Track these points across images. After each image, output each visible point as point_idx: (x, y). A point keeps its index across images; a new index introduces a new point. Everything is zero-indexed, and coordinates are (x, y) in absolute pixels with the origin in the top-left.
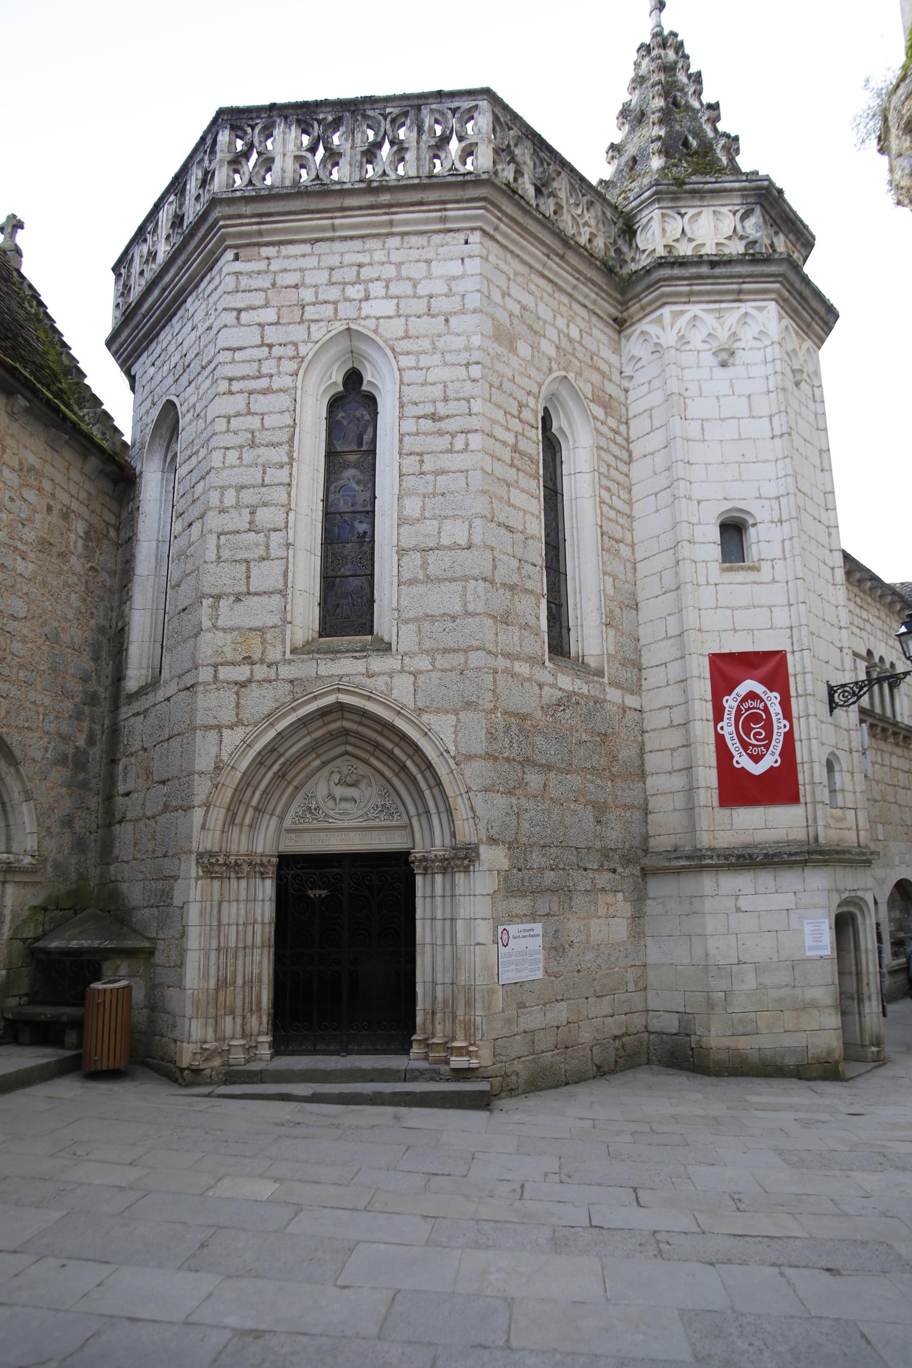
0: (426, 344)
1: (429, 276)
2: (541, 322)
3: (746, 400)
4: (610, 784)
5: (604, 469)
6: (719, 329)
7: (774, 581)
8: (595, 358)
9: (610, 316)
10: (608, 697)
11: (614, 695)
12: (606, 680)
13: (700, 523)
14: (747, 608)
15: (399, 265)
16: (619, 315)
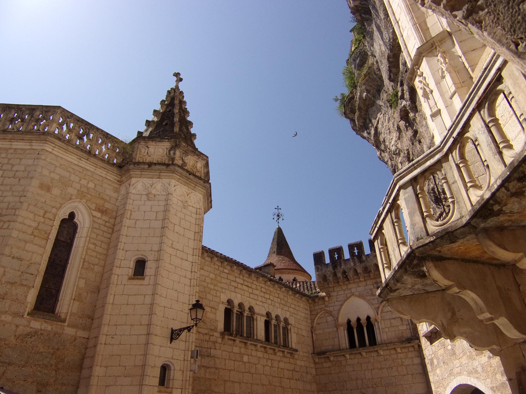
0: (8, 188)
1: (19, 164)
2: (71, 182)
3: (155, 214)
4: (54, 373)
5: (94, 235)
6: (150, 187)
7: (149, 284)
8: (101, 194)
9: (115, 179)
10: (65, 332)
11: (69, 331)
12: (66, 324)
13: (125, 260)
14: (135, 295)
15: (10, 159)
16: (119, 179)
